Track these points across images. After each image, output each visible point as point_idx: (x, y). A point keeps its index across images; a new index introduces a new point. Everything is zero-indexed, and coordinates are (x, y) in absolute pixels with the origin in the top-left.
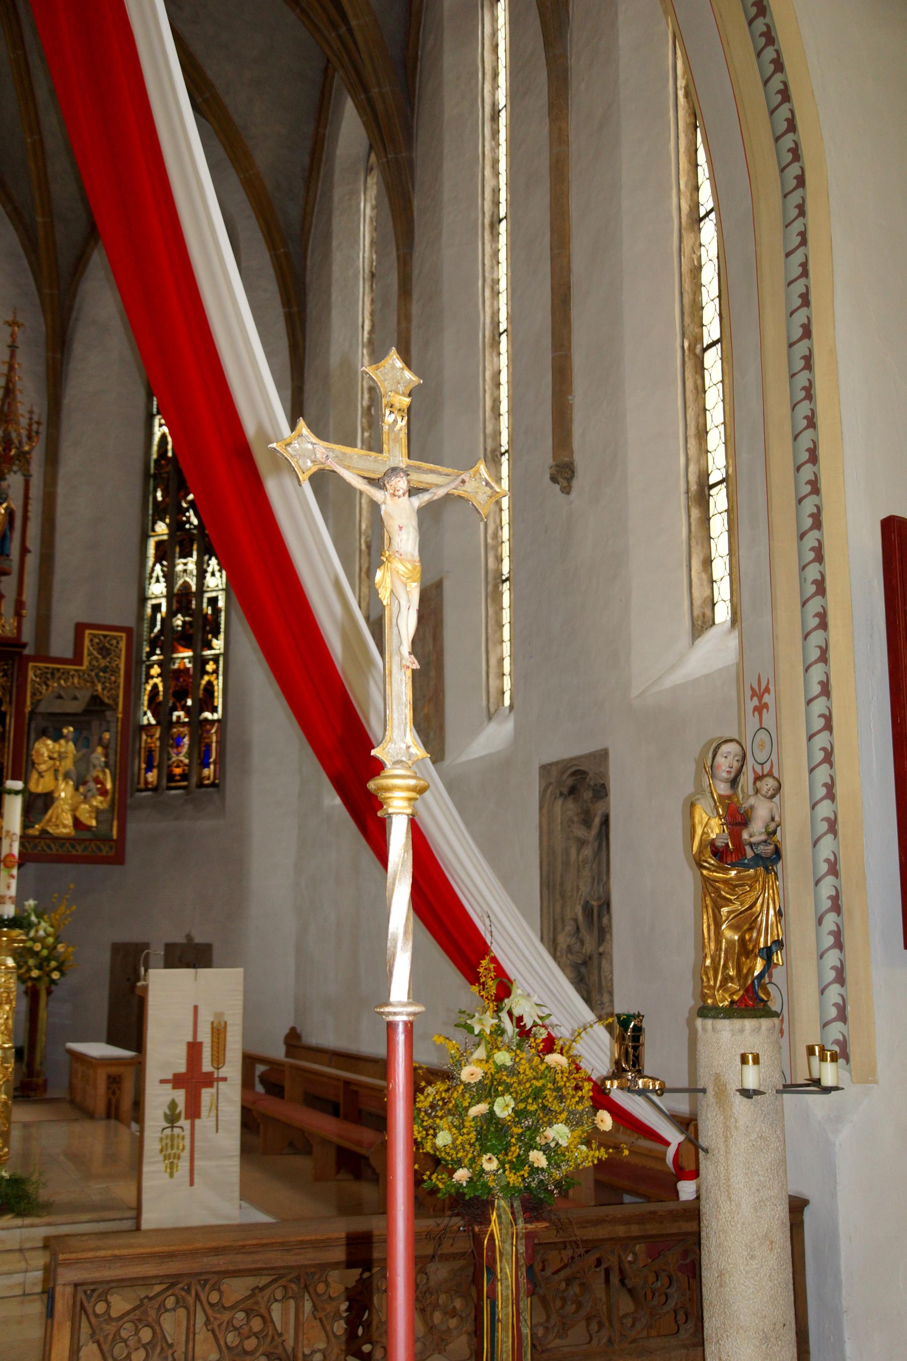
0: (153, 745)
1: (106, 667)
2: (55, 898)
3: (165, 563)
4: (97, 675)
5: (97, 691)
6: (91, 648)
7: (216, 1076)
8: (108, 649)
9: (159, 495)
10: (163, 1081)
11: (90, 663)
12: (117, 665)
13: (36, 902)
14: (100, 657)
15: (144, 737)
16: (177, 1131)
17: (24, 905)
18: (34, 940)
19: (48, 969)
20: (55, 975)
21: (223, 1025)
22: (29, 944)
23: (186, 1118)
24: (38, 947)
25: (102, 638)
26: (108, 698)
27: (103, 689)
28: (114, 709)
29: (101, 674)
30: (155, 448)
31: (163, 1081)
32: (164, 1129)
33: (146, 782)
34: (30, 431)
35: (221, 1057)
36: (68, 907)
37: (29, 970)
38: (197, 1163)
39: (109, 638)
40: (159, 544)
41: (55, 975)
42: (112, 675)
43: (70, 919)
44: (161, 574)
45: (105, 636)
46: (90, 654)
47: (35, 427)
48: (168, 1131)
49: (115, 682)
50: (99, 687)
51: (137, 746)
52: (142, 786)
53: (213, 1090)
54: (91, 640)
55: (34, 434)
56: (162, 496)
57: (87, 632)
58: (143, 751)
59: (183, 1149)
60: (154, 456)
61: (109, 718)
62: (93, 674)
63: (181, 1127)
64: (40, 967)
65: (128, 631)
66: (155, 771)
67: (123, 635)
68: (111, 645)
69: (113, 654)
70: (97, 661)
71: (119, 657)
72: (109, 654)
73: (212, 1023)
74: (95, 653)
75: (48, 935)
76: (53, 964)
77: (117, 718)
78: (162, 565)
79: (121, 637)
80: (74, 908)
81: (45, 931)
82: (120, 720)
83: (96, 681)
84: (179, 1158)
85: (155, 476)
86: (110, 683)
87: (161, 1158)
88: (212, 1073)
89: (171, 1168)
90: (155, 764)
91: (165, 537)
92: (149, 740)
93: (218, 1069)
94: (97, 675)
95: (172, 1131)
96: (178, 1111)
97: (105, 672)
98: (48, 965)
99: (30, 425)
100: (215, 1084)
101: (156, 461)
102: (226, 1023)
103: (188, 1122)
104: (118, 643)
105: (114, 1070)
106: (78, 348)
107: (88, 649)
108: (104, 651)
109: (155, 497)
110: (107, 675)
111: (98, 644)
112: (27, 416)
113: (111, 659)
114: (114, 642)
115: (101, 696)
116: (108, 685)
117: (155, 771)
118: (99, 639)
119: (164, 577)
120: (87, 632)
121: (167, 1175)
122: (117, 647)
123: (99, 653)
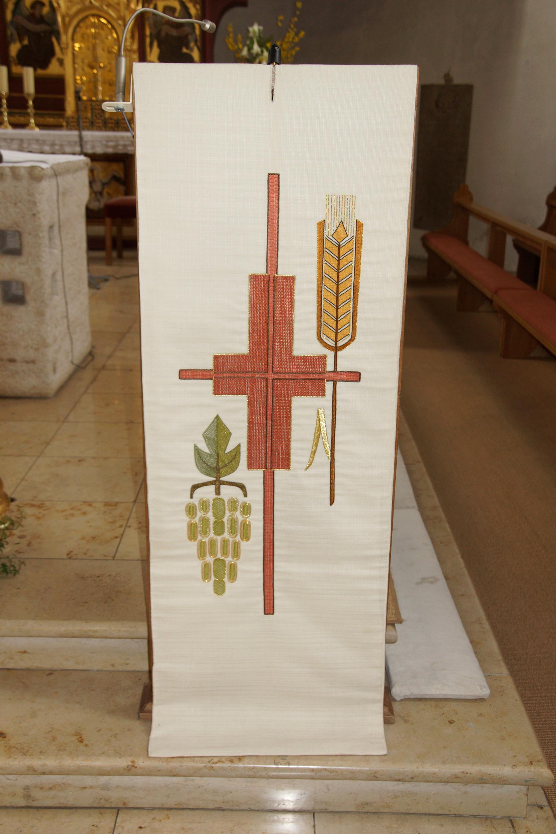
2: (281, 21)
7: (330, 367)
10: (185, 374)
13: (261, 28)
16: (227, 492)
17: (248, 31)
21: (351, 231)
23: (250, 466)
31: (185, 374)
32: (195, 487)
35: (345, 321)
36: (297, 34)
38: (279, 566)
43: (297, 49)
48: (208, 493)
53: (326, 401)
59: (246, 536)
63: (242, 487)
73: (322, 225)
80: (302, 34)
84: (236, 553)
87: (193, 547)
88: (324, 358)
89: (219, 575)
93: (336, 349)
95: (218, 492)
96: (230, 447)
100: (329, 386)
102: (359, 226)
103: (259, 474)
121: (209, 585)
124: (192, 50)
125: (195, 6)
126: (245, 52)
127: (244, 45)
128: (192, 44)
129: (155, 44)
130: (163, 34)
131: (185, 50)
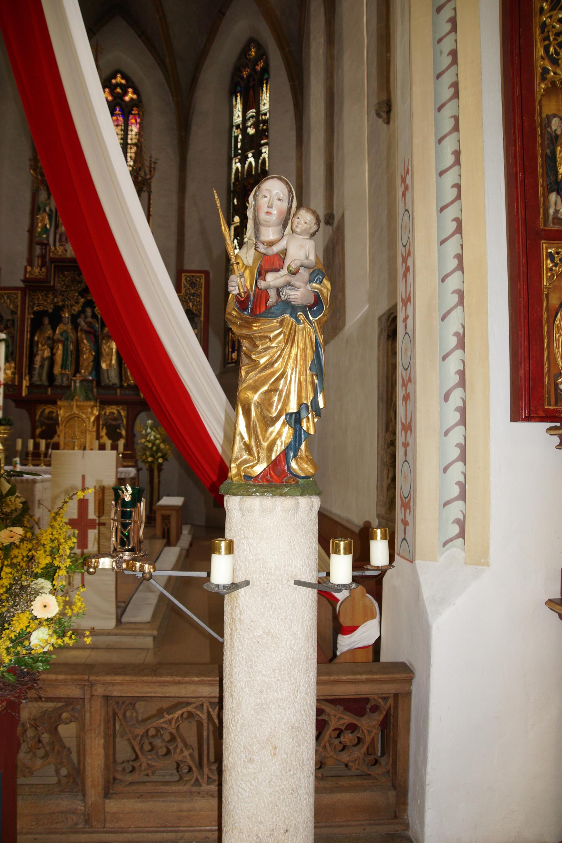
0: (234, 338)
1: (194, 293)
3: (238, 238)
4: (189, 298)
5: (189, 306)
6: (186, 283)
8: (195, 283)
9: (235, 201)
11: (185, 292)
12: (200, 292)
13: (152, 421)
14: (190, 288)
15: (231, 334)
17: (146, 423)
18: (149, 441)
19: (156, 457)
20: (160, 461)
22: (146, 443)
24: (150, 445)
25: (191, 277)
26: (196, 310)
27: (193, 306)
28: (200, 317)
29: (192, 297)
30: (233, 176)
33: (232, 359)
34: (150, 168)
37: (147, 458)
39: (195, 277)
40: (236, 228)
41: (160, 461)
42: (197, 297)
44: (237, 244)
45: (193, 276)
46: (185, 286)
47: (153, 166)
49: (199, 301)
50: (191, 305)
51: (227, 339)
52: (230, 361)
54: (186, 279)
55: (152, 169)
56: (237, 202)
57: (183, 274)
58: (230, 342)
60: (233, 181)
61: (196, 321)
62: (187, 297)
64: (152, 456)
65: (207, 273)
66: (236, 352)
67: (203, 275)
68: (197, 281)
69: (198, 286)
70: (189, 290)
71: (201, 288)
72: (195, 286)
74: (188, 286)
75: (156, 439)
76: (159, 454)
77: (201, 321)
78: (237, 239)
79: (202, 276)
81: (155, 437)
82: (202, 322)
83: (189, 301)
85: (234, 192)
86: (197, 302)
90: (236, 348)
91: (238, 224)
92: (233, 336)
94: (189, 298)
97: (193, 296)
98: (157, 455)
99: (151, 164)
101: (234, 183)
104: (200, 279)
105: (167, 512)
106: (194, 128)
107: (184, 283)
108: (193, 284)
109: (234, 203)
110: (195, 298)
111: (189, 281)
112: (149, 159)
113: (197, 289)
114: (198, 279)
115: (192, 309)
116: (195, 303)
117: (236, 352)
118: (190, 278)
119: (238, 246)
120: (183, 274)
122: (200, 282)
123: (190, 286)
124: (122, 430)
125: (124, 411)
126: (144, 432)
127: (144, 429)
128: (122, 428)
129: (104, 428)
130: (108, 423)
131: (118, 430)
